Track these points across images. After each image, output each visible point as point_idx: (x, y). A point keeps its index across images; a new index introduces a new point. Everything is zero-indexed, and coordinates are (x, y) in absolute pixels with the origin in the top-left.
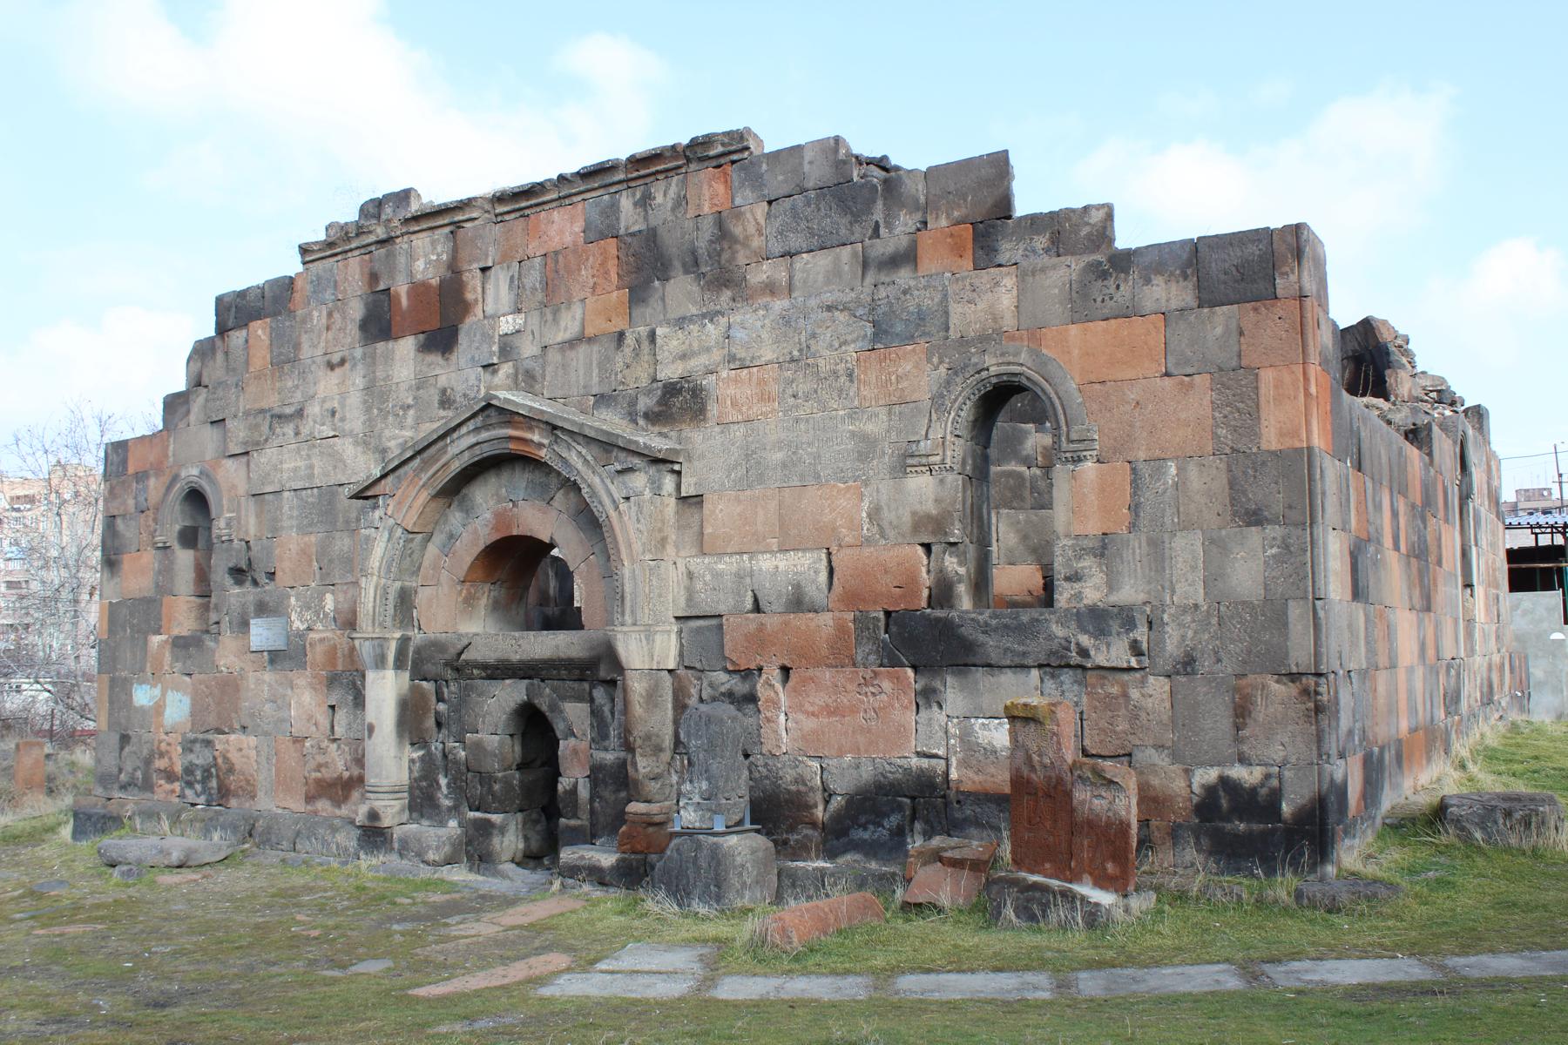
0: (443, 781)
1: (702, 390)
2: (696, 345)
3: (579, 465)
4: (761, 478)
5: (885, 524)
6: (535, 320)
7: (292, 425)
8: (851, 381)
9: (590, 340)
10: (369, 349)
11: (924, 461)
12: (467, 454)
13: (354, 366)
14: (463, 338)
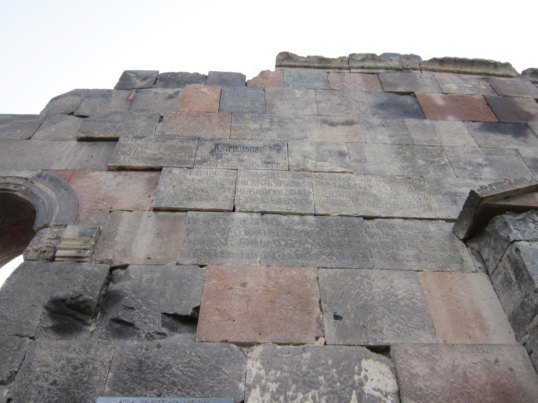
7: (258, 155)
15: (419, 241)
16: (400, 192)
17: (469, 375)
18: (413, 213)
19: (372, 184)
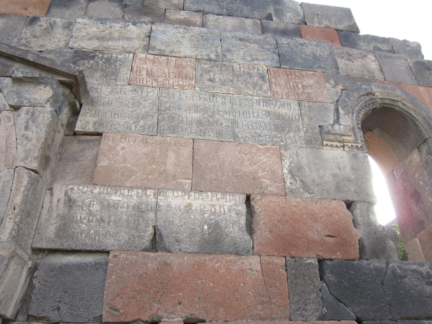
1: (116, 59)
2: (116, 35)
4: (173, 129)
5: (308, 181)
8: (264, 80)
11: (340, 138)
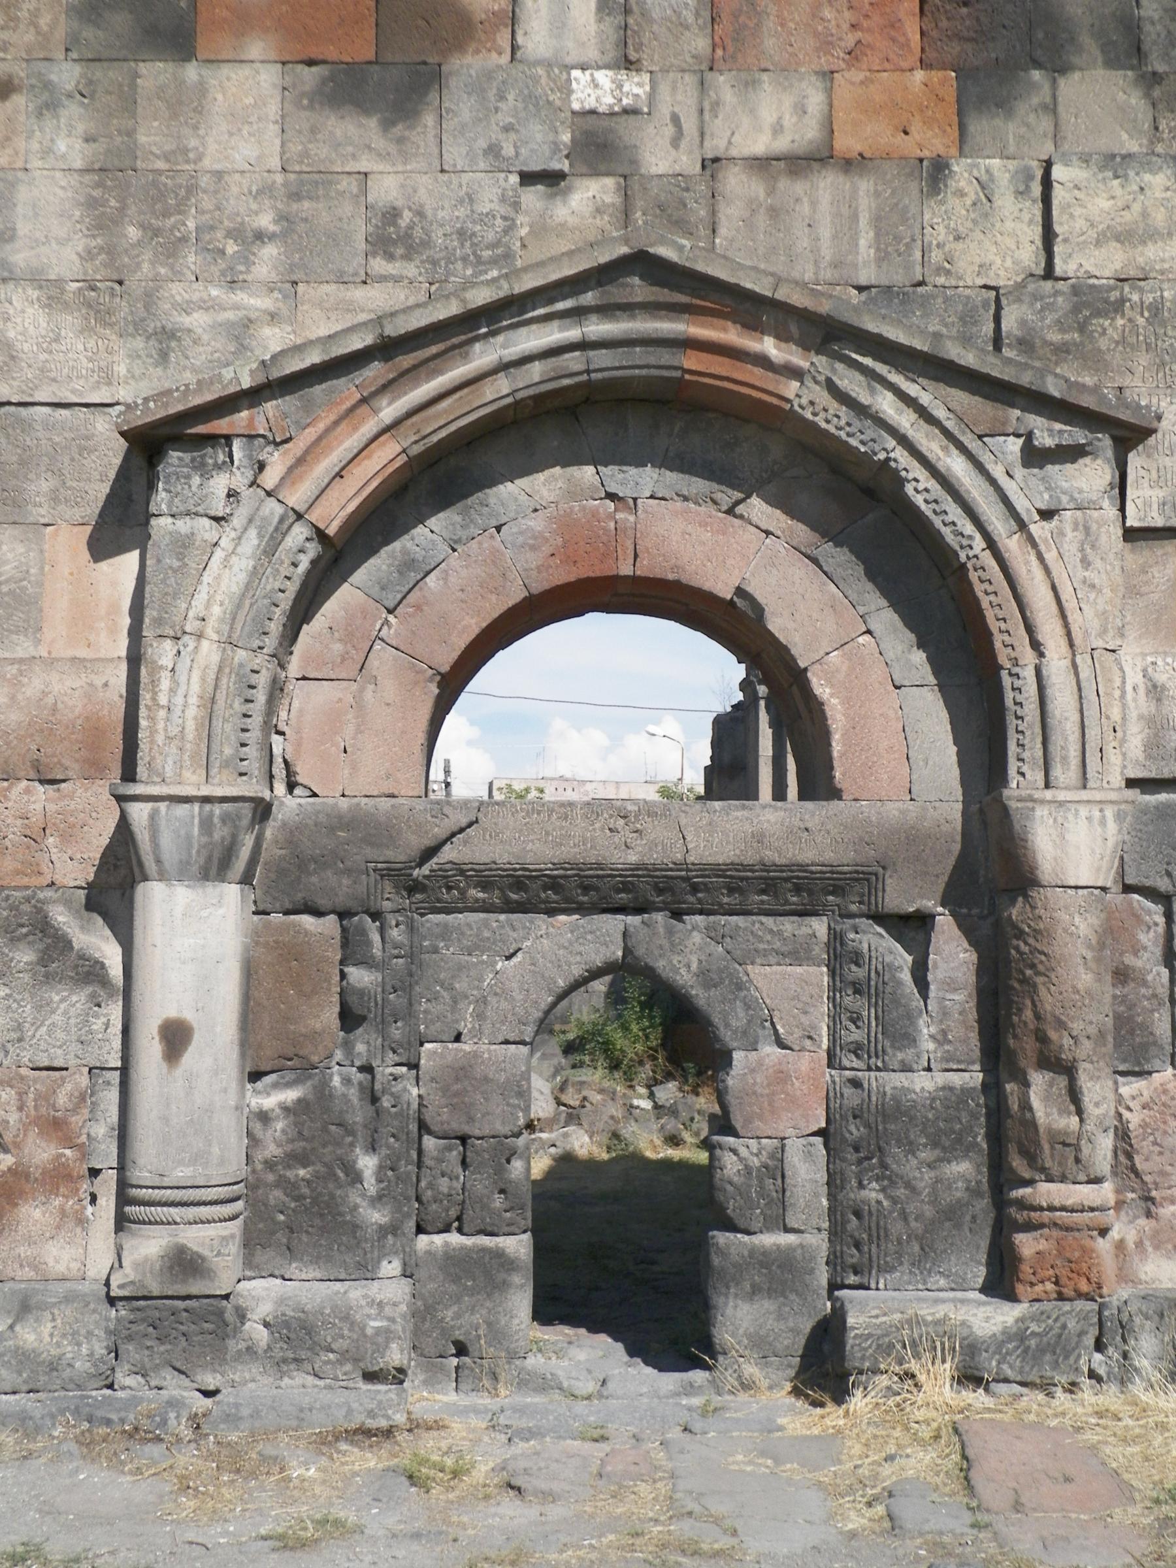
0: (367, 1164)
2: (1159, 217)
3: (905, 420)
6: (679, 97)
9: (852, 165)
10: (113, 74)
12: (536, 370)
13: (49, 105)
14: (460, 104)
15: (66, 460)
16: (63, 333)
17: (60, 706)
18: (73, 391)
19: (11, 312)
